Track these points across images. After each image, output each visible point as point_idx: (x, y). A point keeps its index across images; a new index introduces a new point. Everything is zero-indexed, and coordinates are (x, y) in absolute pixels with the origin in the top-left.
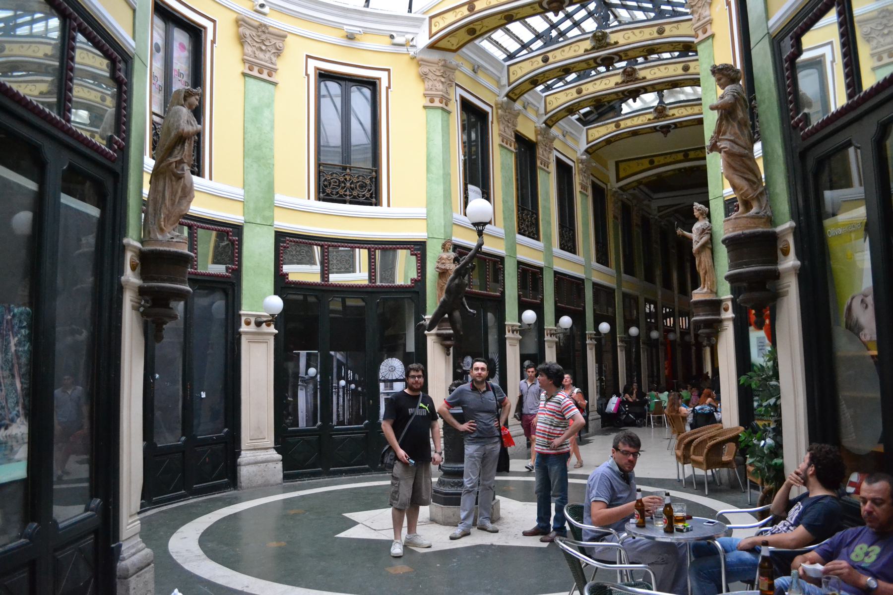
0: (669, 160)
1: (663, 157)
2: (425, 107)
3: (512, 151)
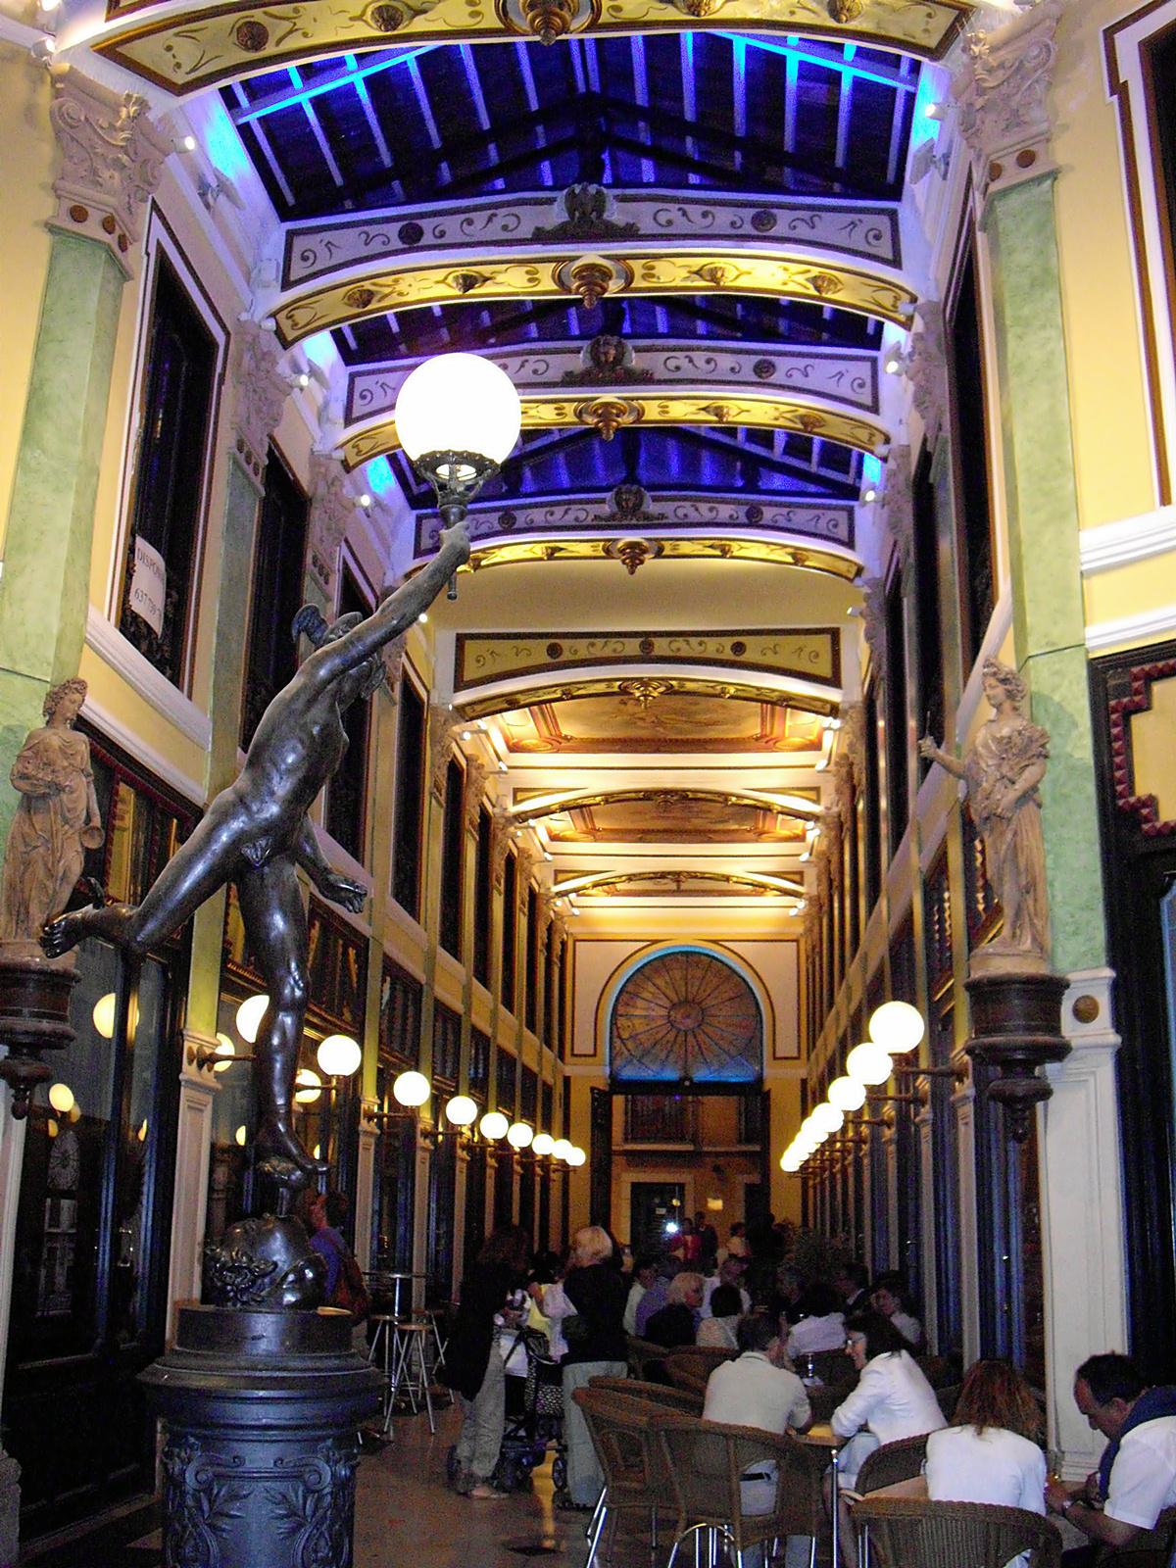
0: (601, 649)
1: (586, 641)
2: (52, 229)
3: (256, 491)
